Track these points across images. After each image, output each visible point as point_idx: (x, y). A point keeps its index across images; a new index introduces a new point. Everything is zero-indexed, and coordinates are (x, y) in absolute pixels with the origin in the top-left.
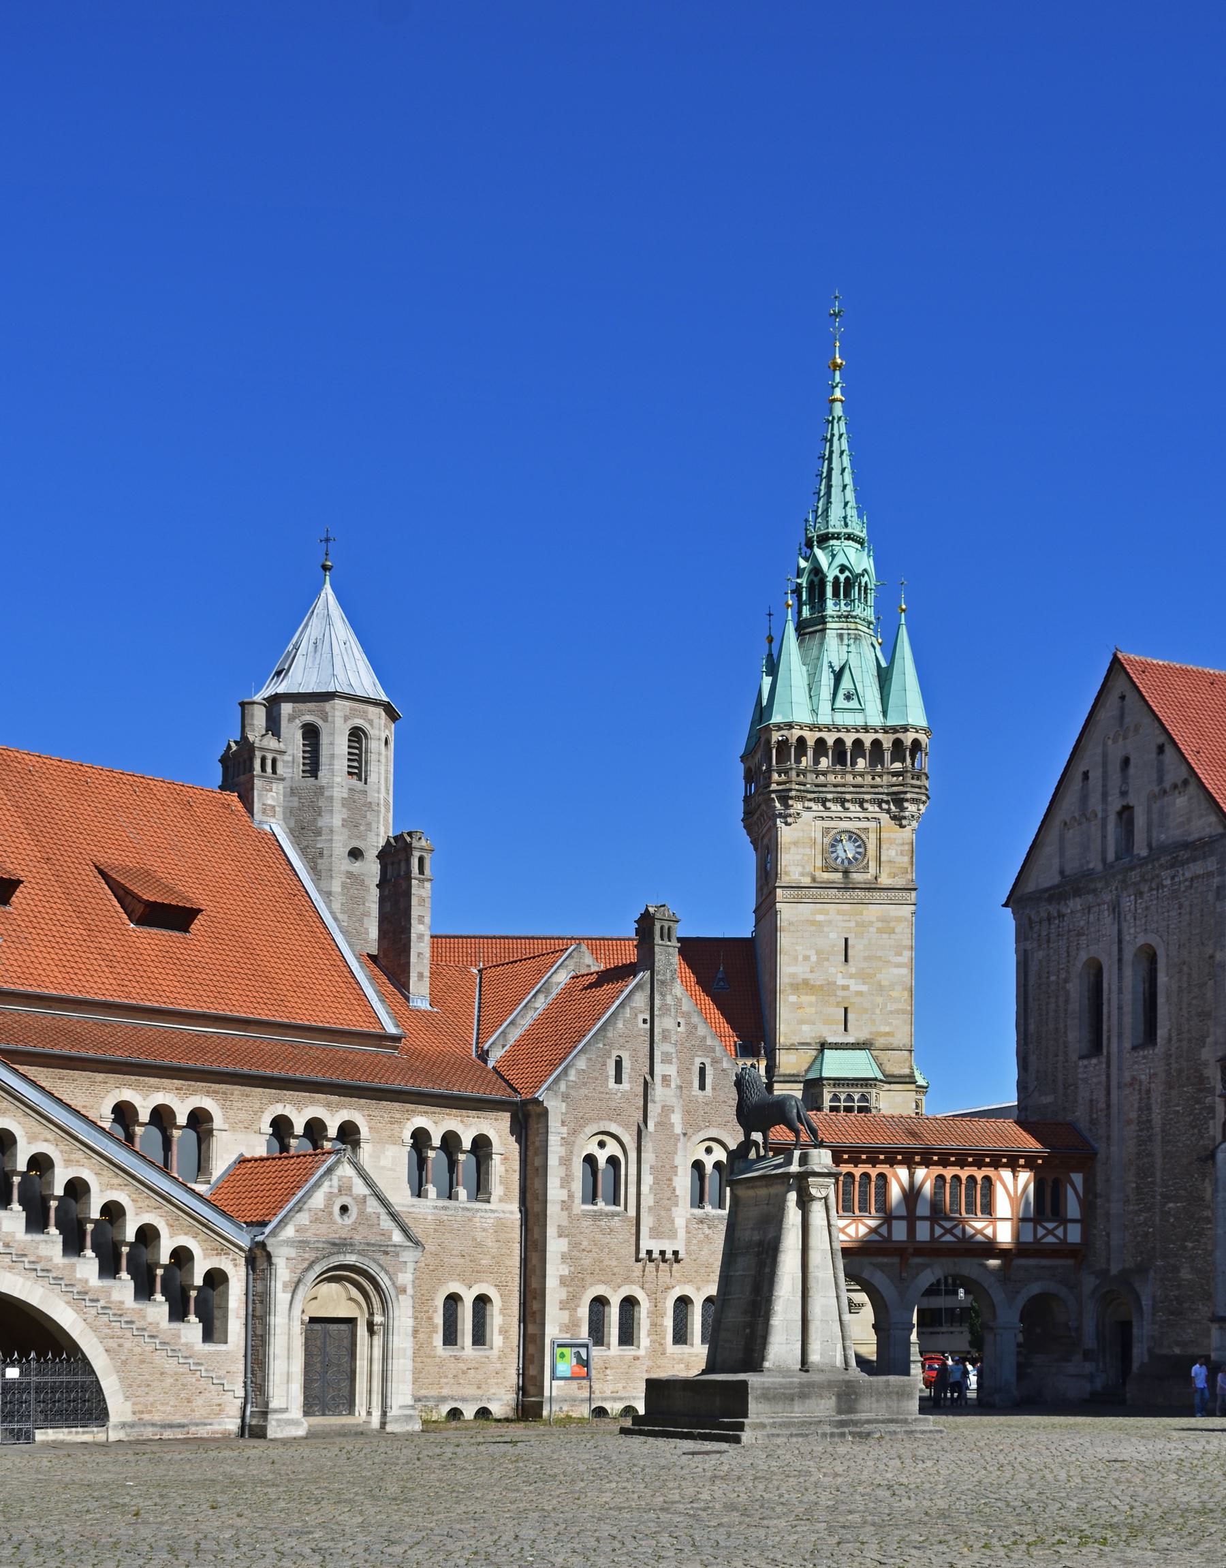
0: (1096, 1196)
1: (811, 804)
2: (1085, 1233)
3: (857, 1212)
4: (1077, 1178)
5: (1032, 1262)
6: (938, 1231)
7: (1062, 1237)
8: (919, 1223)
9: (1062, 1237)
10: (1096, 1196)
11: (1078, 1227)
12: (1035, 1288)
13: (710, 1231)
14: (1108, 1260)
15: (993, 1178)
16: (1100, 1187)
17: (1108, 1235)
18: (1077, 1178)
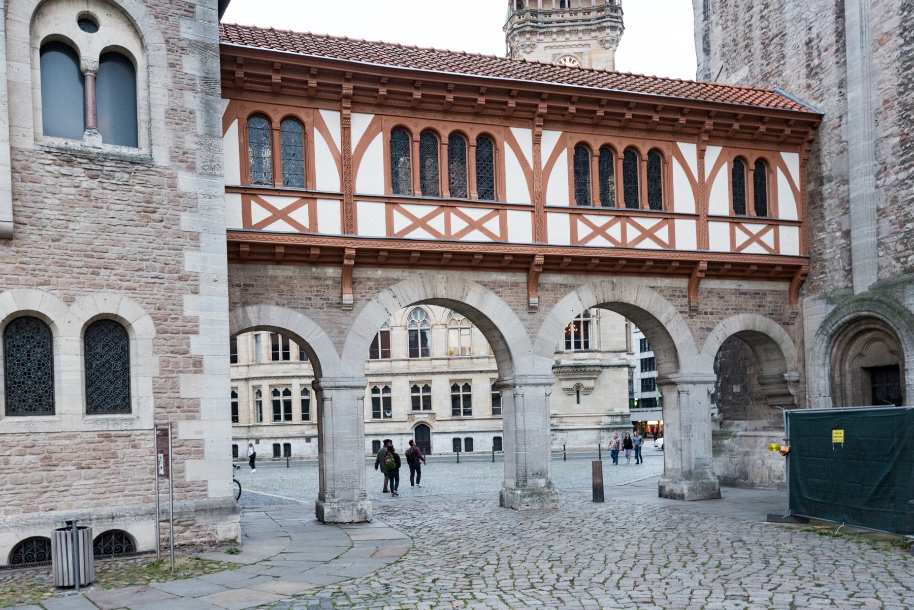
0: (821, 181)
1: (542, 37)
2: (806, 240)
3: (447, 195)
4: (791, 160)
5: (729, 285)
6: (583, 231)
7: (772, 246)
8: (551, 217)
9: (772, 246)
10: (821, 181)
11: (795, 231)
12: (735, 324)
13: (95, 183)
14: (849, 272)
15: (667, 153)
16: (827, 168)
17: (847, 234)
18: (791, 160)
